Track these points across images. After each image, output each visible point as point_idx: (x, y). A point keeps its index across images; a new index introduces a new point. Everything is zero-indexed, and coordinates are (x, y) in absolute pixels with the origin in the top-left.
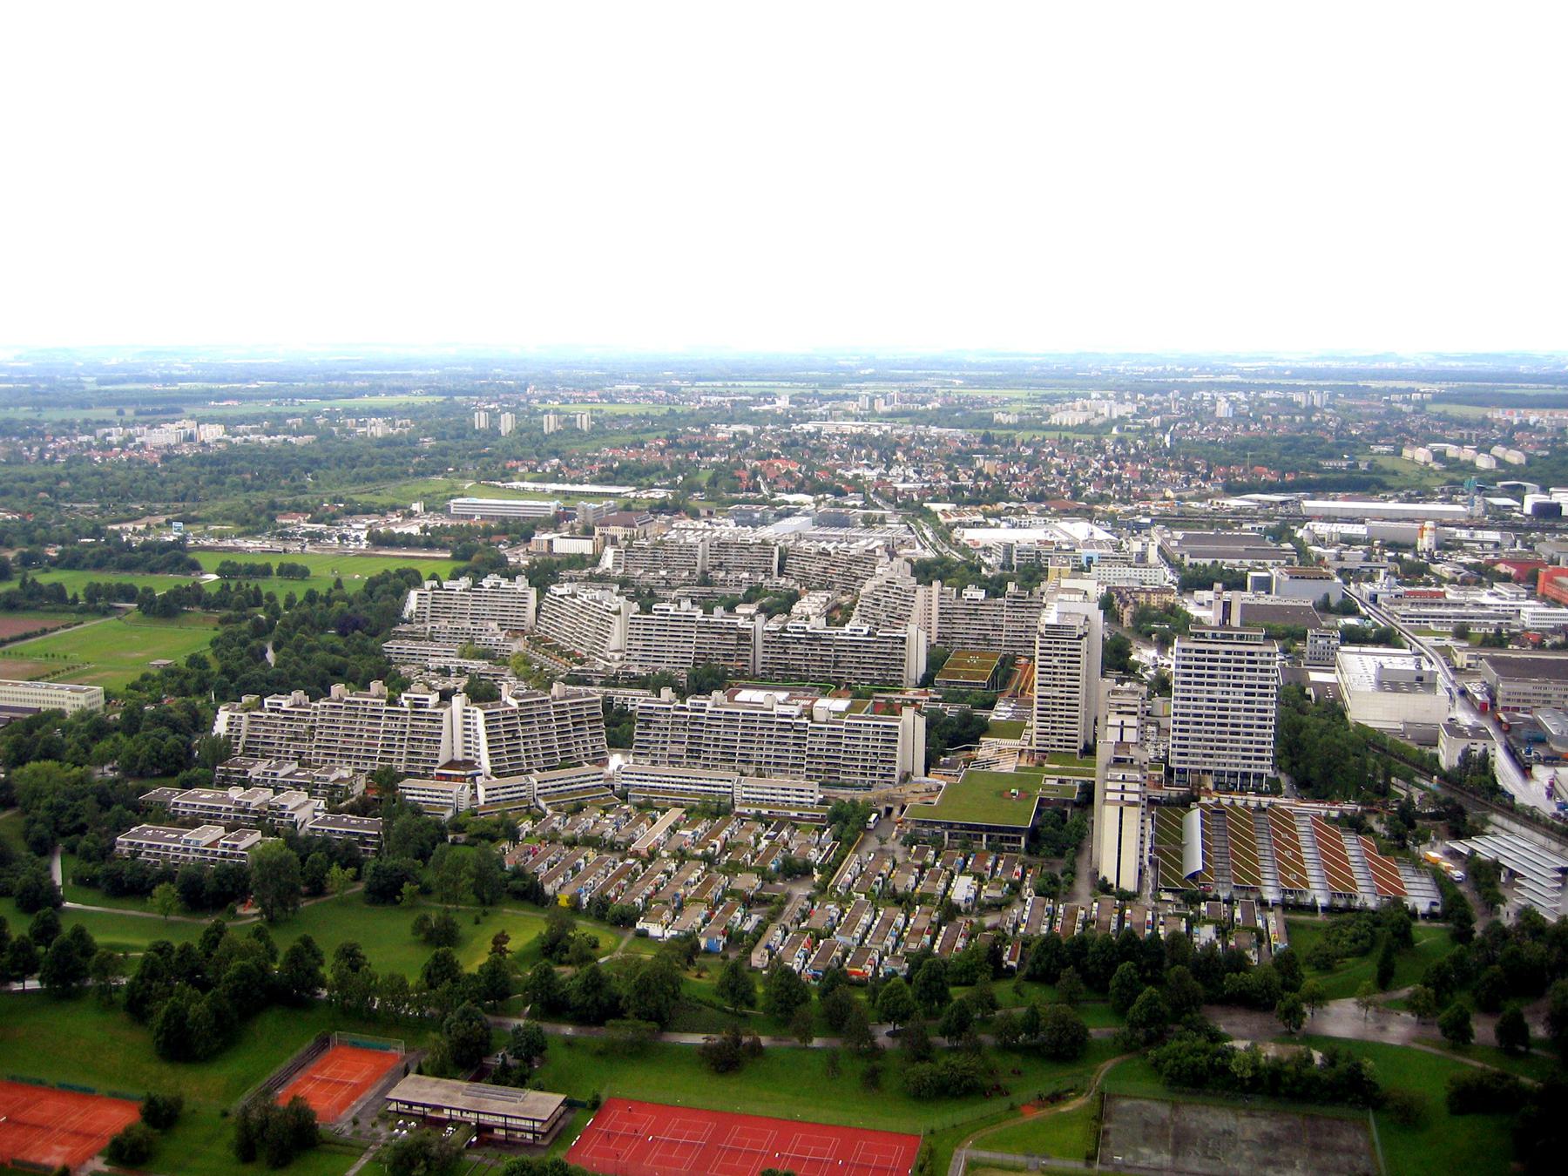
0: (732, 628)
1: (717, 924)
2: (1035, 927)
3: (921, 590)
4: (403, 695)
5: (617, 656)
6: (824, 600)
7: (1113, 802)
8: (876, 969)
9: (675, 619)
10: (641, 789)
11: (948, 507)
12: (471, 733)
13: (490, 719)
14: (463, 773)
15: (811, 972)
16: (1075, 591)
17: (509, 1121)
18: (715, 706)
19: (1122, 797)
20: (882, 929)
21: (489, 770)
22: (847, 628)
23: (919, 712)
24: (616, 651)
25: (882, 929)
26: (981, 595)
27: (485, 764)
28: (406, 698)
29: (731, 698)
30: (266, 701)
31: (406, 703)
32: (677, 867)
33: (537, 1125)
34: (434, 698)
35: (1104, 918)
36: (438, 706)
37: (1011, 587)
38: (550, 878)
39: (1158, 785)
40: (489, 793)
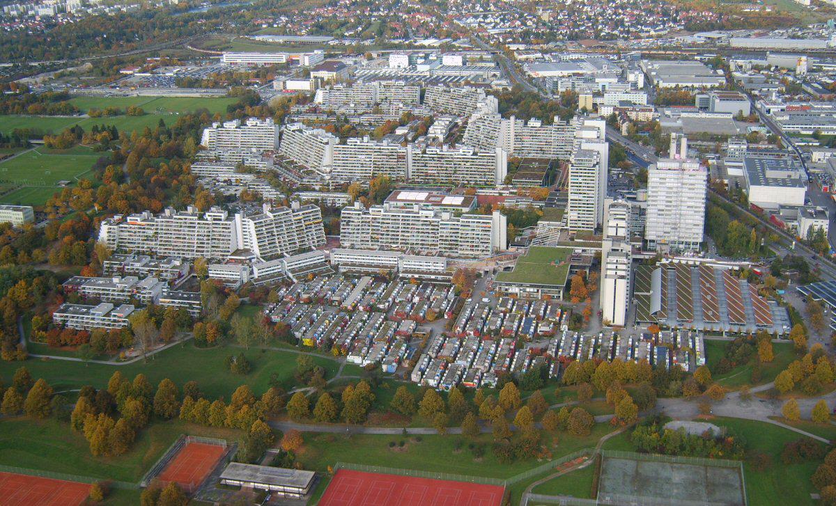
1: (392, 355)
2: (567, 351)
3: (504, 122)
4: (207, 214)
5: (328, 170)
6: (448, 123)
7: (611, 276)
11: (522, 47)
12: (247, 233)
13: (258, 226)
14: (244, 258)
17: (285, 488)
18: (385, 212)
21: (259, 255)
24: (326, 166)
25: (483, 355)
26: (538, 124)
27: (256, 251)
28: (209, 216)
30: (128, 218)
31: (209, 218)
33: (301, 490)
36: (227, 219)
40: (260, 271)
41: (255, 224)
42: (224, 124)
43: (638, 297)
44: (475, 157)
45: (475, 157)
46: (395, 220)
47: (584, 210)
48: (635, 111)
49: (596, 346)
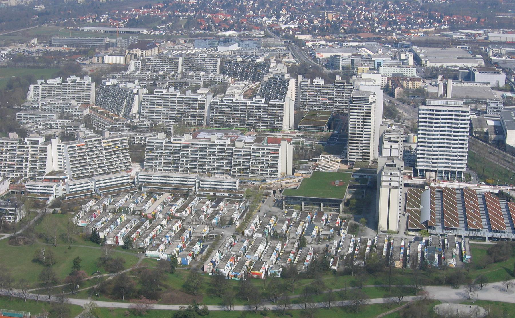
0: (195, 100)
2: (346, 249)
4: (26, 139)
6: (243, 85)
7: (385, 187)
8: (266, 272)
9: (166, 96)
10: (149, 183)
11: (308, 37)
12: (62, 157)
15: (233, 273)
16: (370, 80)
19: (390, 184)
20: (269, 251)
22: (254, 99)
23: (289, 141)
26: (322, 82)
27: (69, 173)
28: (28, 140)
29: (194, 137)
31: (28, 143)
32: (167, 222)
34: (42, 140)
35: (380, 244)
37: (338, 78)
38: (103, 230)
39: (410, 178)
41: (69, 147)
42: (48, 81)
43: (409, 211)
44: (266, 105)
45: (266, 105)
46: (194, 148)
47: (358, 140)
48: (406, 80)
49: (373, 245)
